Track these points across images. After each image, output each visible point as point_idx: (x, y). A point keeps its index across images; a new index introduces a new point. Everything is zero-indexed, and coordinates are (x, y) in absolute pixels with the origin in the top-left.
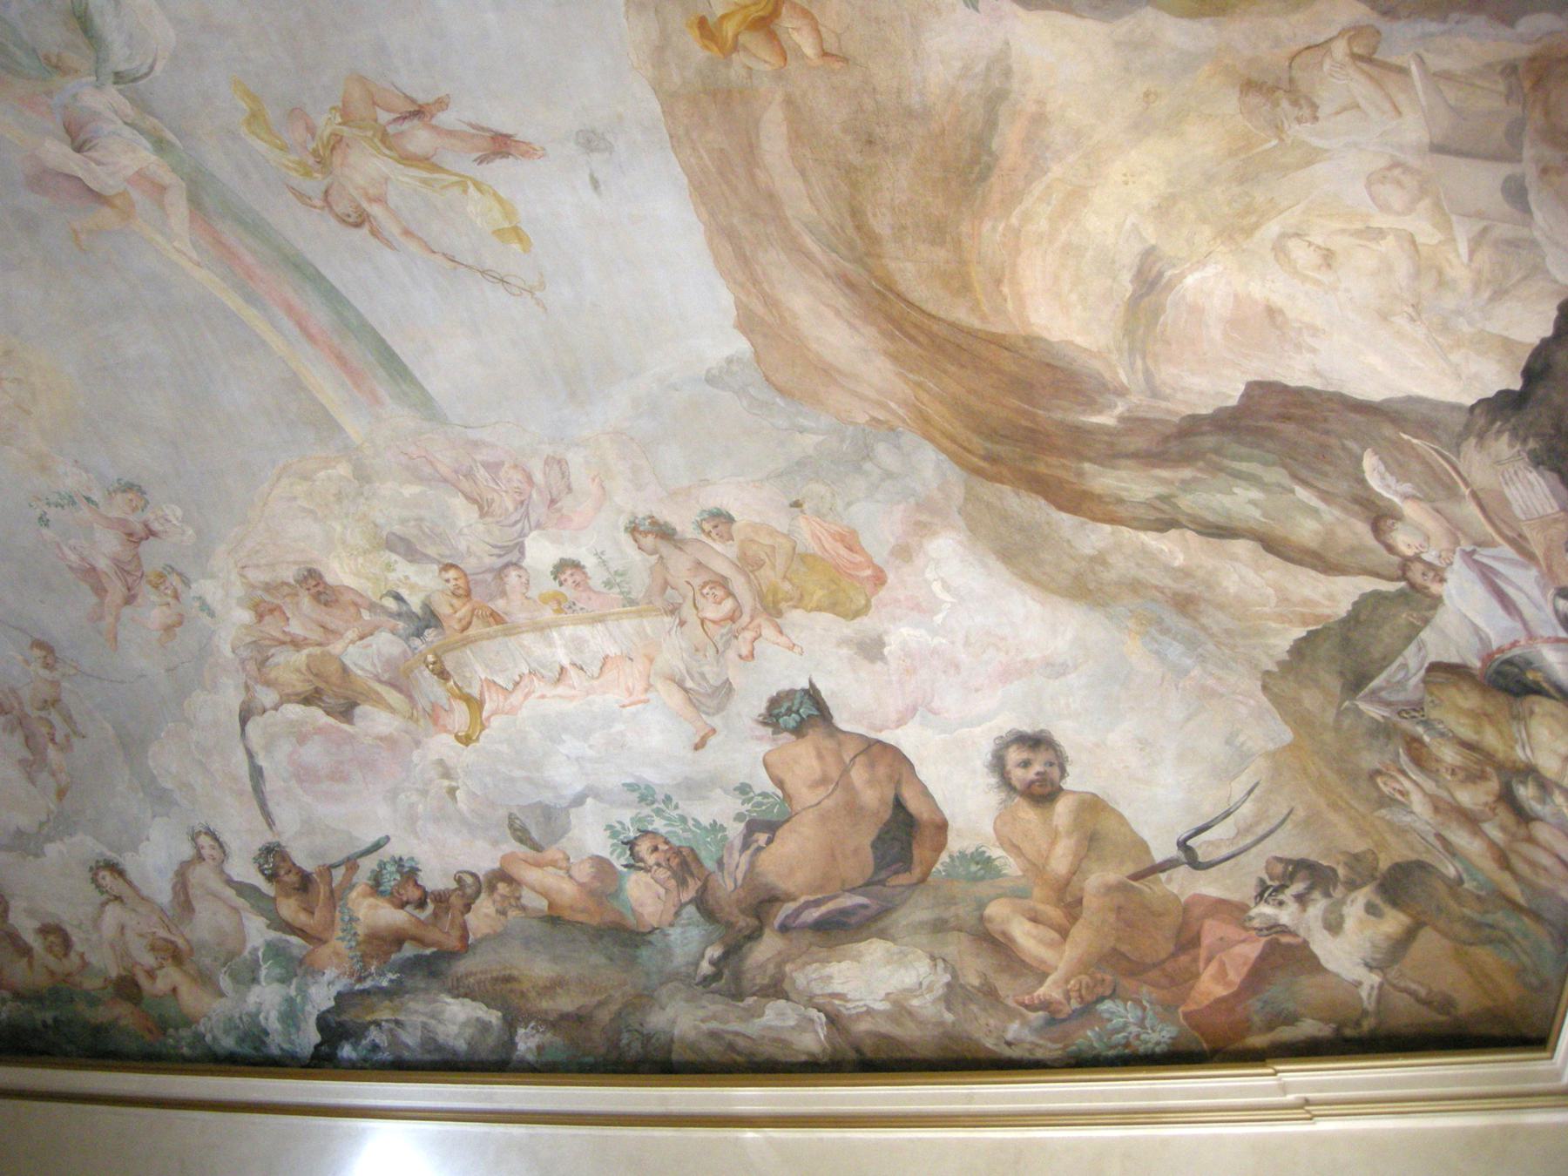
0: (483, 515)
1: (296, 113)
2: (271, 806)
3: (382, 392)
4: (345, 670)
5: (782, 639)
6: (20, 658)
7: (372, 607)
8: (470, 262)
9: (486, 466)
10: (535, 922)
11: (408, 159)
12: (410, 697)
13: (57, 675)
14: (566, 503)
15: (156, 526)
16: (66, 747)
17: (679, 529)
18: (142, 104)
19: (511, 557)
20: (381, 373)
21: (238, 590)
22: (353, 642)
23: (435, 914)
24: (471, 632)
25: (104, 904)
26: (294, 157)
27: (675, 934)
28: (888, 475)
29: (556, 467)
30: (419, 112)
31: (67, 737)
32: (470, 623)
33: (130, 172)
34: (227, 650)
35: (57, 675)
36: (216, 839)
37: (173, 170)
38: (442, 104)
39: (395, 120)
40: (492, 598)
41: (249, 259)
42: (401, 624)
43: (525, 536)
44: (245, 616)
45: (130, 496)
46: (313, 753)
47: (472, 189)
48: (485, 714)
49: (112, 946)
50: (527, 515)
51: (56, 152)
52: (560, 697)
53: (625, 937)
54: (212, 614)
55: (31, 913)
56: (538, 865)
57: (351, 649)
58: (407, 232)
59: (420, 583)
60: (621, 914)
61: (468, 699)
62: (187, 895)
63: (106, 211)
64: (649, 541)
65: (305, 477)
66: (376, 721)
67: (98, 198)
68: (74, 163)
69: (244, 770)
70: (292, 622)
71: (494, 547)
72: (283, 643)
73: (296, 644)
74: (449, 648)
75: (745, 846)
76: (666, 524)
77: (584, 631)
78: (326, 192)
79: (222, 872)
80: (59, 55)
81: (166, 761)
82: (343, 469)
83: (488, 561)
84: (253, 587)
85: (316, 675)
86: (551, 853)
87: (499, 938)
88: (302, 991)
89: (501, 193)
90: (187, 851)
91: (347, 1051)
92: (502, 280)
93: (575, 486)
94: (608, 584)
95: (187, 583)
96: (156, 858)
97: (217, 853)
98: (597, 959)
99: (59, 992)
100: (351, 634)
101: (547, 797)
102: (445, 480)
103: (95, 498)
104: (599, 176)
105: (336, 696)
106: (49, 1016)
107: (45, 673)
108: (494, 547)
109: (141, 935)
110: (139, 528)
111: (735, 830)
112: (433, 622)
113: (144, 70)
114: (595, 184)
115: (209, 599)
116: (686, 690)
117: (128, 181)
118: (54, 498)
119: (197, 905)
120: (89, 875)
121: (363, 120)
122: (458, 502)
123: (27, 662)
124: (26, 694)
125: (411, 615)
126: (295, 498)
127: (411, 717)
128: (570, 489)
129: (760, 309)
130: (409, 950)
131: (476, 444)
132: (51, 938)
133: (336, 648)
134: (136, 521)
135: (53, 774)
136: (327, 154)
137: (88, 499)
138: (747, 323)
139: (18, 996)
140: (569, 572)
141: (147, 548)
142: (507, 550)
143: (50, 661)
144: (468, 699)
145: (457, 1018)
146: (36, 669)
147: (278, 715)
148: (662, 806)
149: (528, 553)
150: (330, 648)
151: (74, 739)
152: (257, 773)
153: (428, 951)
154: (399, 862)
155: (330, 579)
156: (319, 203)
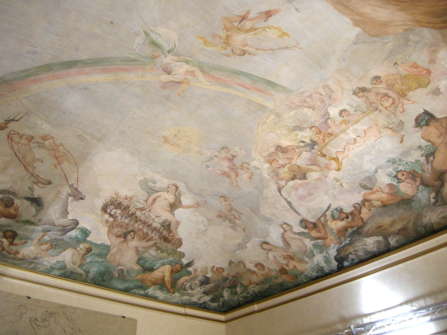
0: (314, 110)
1: (214, 36)
2: (297, 209)
3: (272, 92)
4: (299, 167)
5: (410, 102)
6: (218, 202)
7: (298, 147)
8: (277, 48)
9: (308, 97)
10: (380, 209)
11: (247, 31)
12: (319, 166)
13: (229, 202)
14: (333, 96)
15: (234, 154)
16: (240, 219)
17: (367, 87)
18: (178, 55)
19: (326, 117)
20: (270, 87)
21: (262, 160)
22: (297, 159)
23: (352, 218)
24: (326, 141)
25: (267, 253)
26: (220, 47)
27: (419, 195)
28: (417, 43)
29: (326, 88)
30: (244, 18)
31: (239, 216)
32: (324, 140)
33: (184, 72)
34: (267, 176)
35: (229, 202)
36: (287, 224)
37: (193, 66)
38: (248, 13)
39: (239, 23)
40: (327, 130)
41: (223, 78)
42: (307, 148)
43: (327, 109)
44: (267, 165)
45: (224, 150)
46: (301, 191)
47: (267, 30)
48: (340, 160)
49: (274, 262)
50: (325, 104)
51: (165, 78)
52: (357, 146)
53: (406, 202)
54: (259, 169)
55: (251, 263)
56: (373, 193)
57: (297, 161)
58: (257, 49)
59: (307, 135)
60: (402, 196)
61: (333, 159)
62: (287, 241)
63: (183, 85)
64: (361, 94)
65: (265, 123)
66: (313, 176)
67: (180, 83)
69: (286, 204)
70: (279, 161)
71: (321, 116)
72: (280, 167)
73: (283, 166)
74: (323, 148)
75: (428, 162)
76: (363, 87)
77: (355, 126)
78: (232, 50)
79: (293, 232)
80: (153, 55)
81: (266, 211)
82: (273, 116)
83: (321, 121)
84: (266, 157)
85: (292, 171)
86: (375, 188)
87: (372, 217)
88: (327, 253)
89: (275, 26)
90: (282, 231)
91: (346, 264)
92: (287, 48)
93: (334, 90)
94: (355, 111)
95: (249, 164)
96: (275, 236)
97: (289, 228)
98: (401, 211)
99: (267, 279)
100: (296, 157)
101: (367, 174)
102: (299, 106)
103: (216, 155)
104: (297, 7)
105: (300, 174)
106: (267, 286)
107: (225, 203)
108: (321, 116)
109: (280, 257)
110: (230, 157)
111: (423, 159)
112: (315, 144)
113: (174, 46)
114: (297, 10)
115: (256, 166)
116: (391, 128)
117: (184, 75)
118: (207, 160)
119: (291, 243)
120: (260, 247)
121: (231, 28)
122: (306, 110)
123: (220, 202)
124: (224, 210)
125: (308, 145)
126: (265, 130)
127: (322, 171)
128: (333, 92)
129: (357, 18)
130: (350, 231)
131: (303, 93)
132: (259, 267)
133: (294, 162)
134: (229, 155)
135: (240, 226)
136: (227, 42)
137: (215, 156)
138: (356, 23)
139: (257, 284)
140: (343, 113)
141: (235, 161)
142: (324, 116)
143: (226, 199)
144: (333, 159)
145: (371, 243)
146: (224, 203)
147: (288, 186)
148: (399, 162)
149: (330, 113)
150: (292, 163)
151: (241, 216)
152: (289, 203)
153: (355, 229)
154: (336, 209)
155: (283, 146)
156: (232, 54)
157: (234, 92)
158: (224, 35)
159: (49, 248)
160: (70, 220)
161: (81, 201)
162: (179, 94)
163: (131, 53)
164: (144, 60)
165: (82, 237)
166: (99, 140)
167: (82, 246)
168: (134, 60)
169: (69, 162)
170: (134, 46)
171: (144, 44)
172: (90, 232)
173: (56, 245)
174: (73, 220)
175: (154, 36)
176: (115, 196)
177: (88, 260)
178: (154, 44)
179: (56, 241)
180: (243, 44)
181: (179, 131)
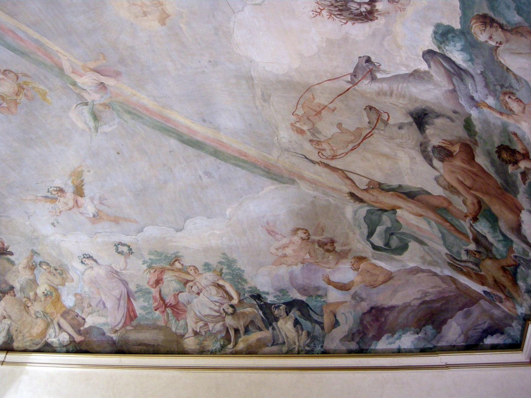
26: (30, 86)
33: (85, 77)
51: (110, 82)
67: (96, 71)
68: (103, 79)
78: (18, 78)
80: (105, 108)
113: (78, 106)
156: (20, 75)
157: (30, 32)
158: (21, 96)
159: (514, 98)
160: (429, 66)
161: (373, 59)
162: (104, 59)
163: (125, 121)
164: (118, 108)
165: (456, 39)
166: (250, 79)
167: (483, 37)
168: (129, 113)
169: (314, 98)
170: (114, 127)
171: (105, 124)
172: (438, 26)
173: (502, 86)
174: (426, 61)
175: (92, 124)
176: (325, 13)
177: (517, 19)
178: (96, 117)
179: (492, 87)
180: (3, 82)
181: (137, 17)
